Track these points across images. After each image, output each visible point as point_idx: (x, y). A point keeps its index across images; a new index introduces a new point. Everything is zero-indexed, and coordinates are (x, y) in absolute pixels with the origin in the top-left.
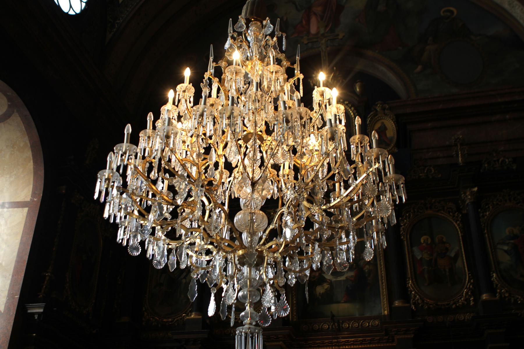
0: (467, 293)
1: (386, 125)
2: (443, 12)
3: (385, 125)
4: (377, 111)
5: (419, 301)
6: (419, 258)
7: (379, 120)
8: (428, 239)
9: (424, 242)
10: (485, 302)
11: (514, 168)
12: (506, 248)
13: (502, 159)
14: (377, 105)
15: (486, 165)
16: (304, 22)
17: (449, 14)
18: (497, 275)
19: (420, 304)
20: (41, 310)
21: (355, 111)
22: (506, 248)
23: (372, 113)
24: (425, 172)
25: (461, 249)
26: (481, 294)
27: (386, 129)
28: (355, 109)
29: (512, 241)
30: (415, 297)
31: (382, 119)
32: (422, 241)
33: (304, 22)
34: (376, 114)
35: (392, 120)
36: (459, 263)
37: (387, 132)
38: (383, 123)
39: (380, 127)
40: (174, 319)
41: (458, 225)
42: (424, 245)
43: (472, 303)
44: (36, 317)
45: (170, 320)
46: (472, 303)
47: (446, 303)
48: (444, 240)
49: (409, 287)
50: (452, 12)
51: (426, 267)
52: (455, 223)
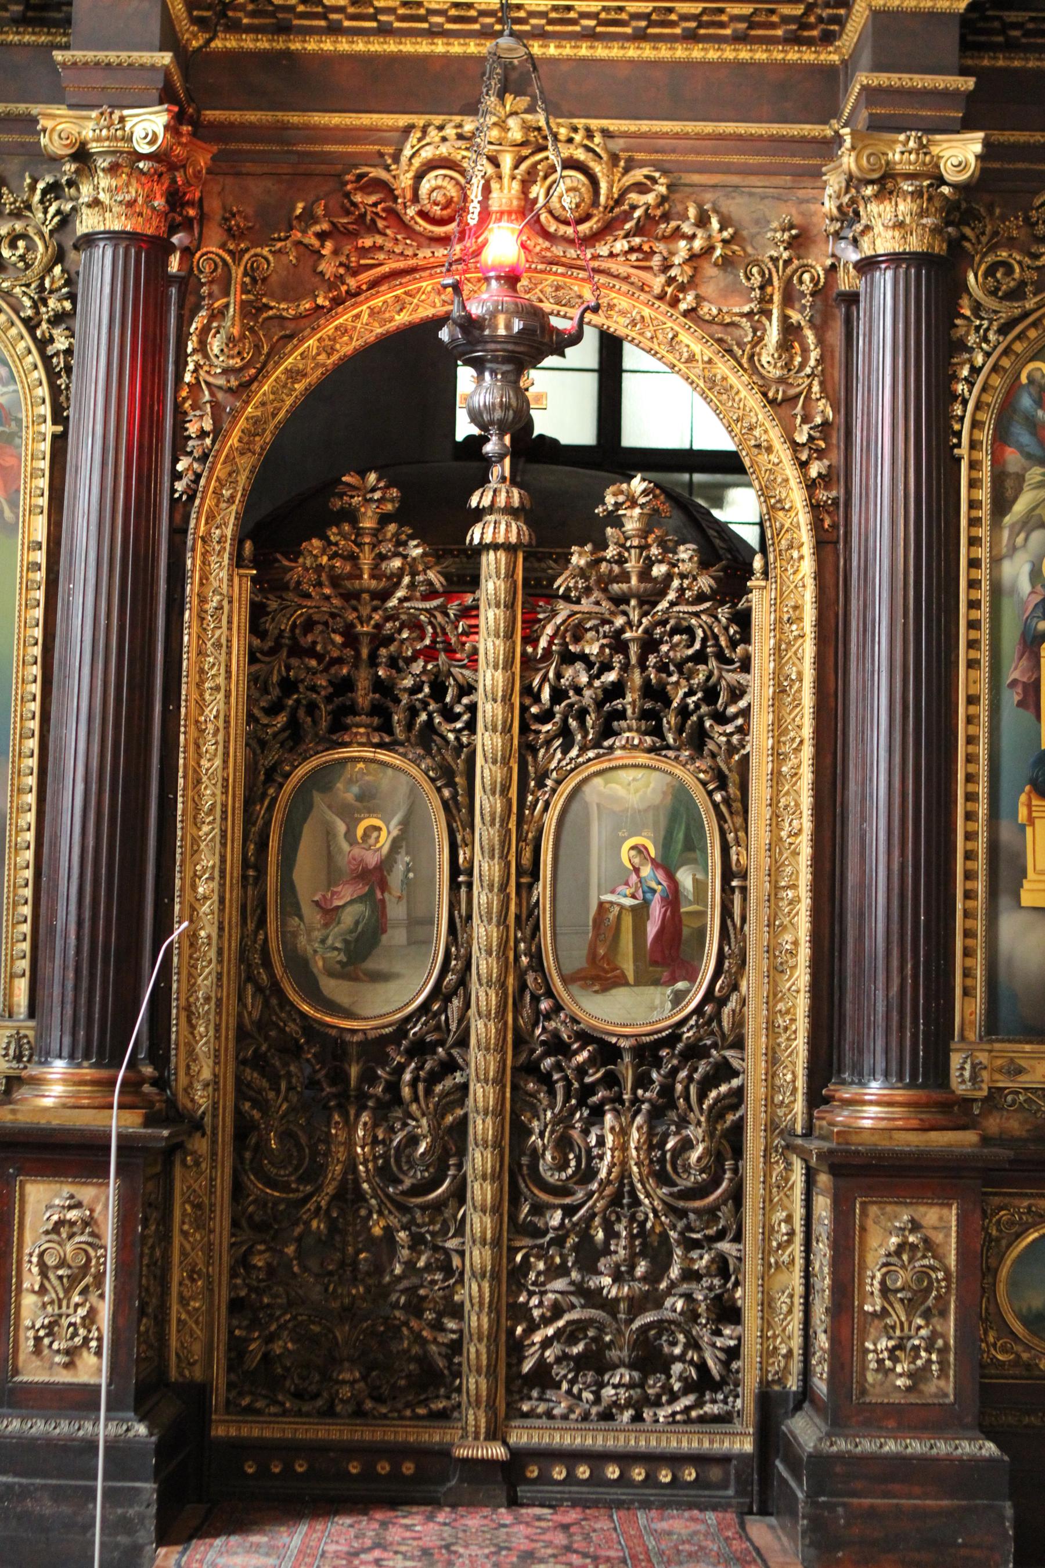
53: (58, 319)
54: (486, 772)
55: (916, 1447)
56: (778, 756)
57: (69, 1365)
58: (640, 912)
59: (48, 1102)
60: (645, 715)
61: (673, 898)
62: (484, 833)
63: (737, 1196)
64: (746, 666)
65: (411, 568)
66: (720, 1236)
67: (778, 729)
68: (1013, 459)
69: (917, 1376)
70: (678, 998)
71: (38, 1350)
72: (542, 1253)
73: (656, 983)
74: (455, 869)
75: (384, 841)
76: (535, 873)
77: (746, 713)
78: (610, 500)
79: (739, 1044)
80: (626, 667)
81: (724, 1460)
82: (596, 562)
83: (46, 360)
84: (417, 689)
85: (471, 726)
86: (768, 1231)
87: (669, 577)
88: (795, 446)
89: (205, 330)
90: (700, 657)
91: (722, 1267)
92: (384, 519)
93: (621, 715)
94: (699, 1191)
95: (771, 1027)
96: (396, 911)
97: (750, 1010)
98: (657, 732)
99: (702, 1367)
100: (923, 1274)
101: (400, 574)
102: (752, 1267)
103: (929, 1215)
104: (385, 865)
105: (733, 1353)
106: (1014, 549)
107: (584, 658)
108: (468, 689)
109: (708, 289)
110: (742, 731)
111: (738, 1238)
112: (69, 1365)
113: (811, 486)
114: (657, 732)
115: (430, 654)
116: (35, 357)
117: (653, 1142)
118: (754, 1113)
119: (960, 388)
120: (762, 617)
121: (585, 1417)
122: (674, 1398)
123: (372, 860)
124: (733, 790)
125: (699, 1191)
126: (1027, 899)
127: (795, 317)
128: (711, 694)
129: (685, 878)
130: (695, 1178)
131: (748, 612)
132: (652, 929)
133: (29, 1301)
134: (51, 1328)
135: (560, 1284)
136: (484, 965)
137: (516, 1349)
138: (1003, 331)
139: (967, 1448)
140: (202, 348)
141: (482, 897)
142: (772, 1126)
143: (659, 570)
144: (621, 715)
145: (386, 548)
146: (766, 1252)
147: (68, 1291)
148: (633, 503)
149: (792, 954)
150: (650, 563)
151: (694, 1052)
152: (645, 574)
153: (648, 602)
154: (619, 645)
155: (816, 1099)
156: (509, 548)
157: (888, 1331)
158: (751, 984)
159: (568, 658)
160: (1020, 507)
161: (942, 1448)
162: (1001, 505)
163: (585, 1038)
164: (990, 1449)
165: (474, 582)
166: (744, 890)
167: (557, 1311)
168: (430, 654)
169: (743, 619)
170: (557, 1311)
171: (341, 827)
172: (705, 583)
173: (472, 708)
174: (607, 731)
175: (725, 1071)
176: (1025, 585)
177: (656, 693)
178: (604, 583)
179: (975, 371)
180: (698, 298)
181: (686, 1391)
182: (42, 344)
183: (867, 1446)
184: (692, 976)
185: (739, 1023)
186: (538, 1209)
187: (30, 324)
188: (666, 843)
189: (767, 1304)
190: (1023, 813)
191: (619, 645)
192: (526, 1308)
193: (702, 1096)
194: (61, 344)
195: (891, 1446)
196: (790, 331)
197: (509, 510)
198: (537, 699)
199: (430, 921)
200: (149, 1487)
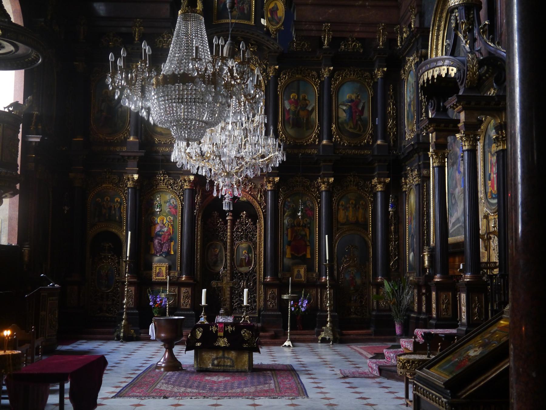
0: (315, 136)
3: (277, 6)
5: (284, 139)
6: (288, 109)
8: (295, 96)
9: (293, 98)
10: (324, 145)
11: (361, 51)
12: (345, 108)
13: (355, 43)
15: (343, 47)
18: (336, 125)
19: (284, 140)
20: (38, 140)
22: (345, 108)
25: (316, 105)
26: (323, 140)
27: (277, 9)
29: (349, 104)
30: (282, 135)
32: (291, 97)
35: (283, 2)
36: (313, 116)
37: (278, 12)
38: (276, 4)
39: (274, 7)
40: (114, 138)
41: (317, 88)
42: (293, 100)
43: (317, 143)
44: (34, 144)
45: (111, 138)
46: (317, 143)
47: (301, 141)
48: (306, 98)
49: (279, 128)
51: (291, 116)
52: (315, 87)
53: (181, 195)
54: (228, 244)
55: (273, 313)
56: (260, 242)
57: (186, 306)
58: (245, 259)
59: (183, 279)
60: (245, 238)
61: (249, 257)
62: (228, 251)
63: (256, 288)
64: (256, 232)
65: (220, 222)
66: (254, 294)
67: (260, 239)
68: (285, 209)
69: (273, 306)
70: (250, 268)
71: (183, 305)
72: (235, 296)
73: (247, 266)
74: (225, 255)
75: (218, 251)
76: (234, 255)
77: (256, 237)
78: (242, 214)
79: (256, 273)
80: (243, 232)
81: (255, 317)
82: (240, 221)
83: (180, 200)
84: (221, 235)
85: (227, 239)
86: (259, 293)
87: (248, 222)
88: (261, 208)
89: (197, 196)
90: (252, 231)
91: (254, 297)
92: (217, 217)
93: (243, 238)
94: (252, 288)
95: (259, 271)
96: (219, 259)
97: (257, 269)
98: (247, 239)
99: (252, 307)
100: (273, 296)
101: (219, 222)
102: (257, 297)
103: (274, 290)
104: (218, 254)
105: (256, 306)
106: (285, 219)
107: (239, 231)
108: (227, 235)
109: (252, 191)
110: (256, 239)
111: (256, 294)
112: (186, 306)
113: (263, 212)
114: (247, 239)
115: (222, 231)
116: (179, 199)
117: (247, 284)
118: (257, 280)
119: (280, 201)
120: (258, 227)
121: (240, 313)
122: (249, 311)
123: (216, 254)
124: (255, 246)
125: (252, 288)
126: (287, 257)
127: (262, 194)
128: (253, 235)
129: (250, 255)
130: (252, 287)
131: (257, 226)
132: (247, 261)
133: (182, 300)
134: (184, 303)
135: (237, 299)
136: (228, 265)
137: (233, 306)
138: (284, 195)
139: (278, 313)
140: (197, 198)
141: (228, 257)
142: (260, 282)
143: (247, 222)
144: (243, 238)
145: (217, 220)
146: (259, 295)
147: (186, 299)
148: (244, 215)
149: (262, 263)
150: (246, 221)
151: (251, 274)
152: (245, 222)
153: (246, 225)
154: (242, 230)
155: (264, 279)
156: (230, 220)
157: (270, 302)
158: (257, 266)
159: (237, 231)
160: (286, 214)
161: (275, 313)
162: (284, 214)
163: (240, 272)
164: (280, 313)
165: (227, 223)
166: (256, 256)
167: (237, 302)
168: (222, 231)
169: (256, 227)
170: (237, 302)
171: (213, 250)
172: (252, 223)
173: (227, 237)
174: (242, 239)
175: (255, 276)
176: (286, 223)
177: (247, 235)
178: (241, 223)
179: (281, 200)
180: (251, 192)
181: (250, 310)
182: (180, 198)
183: (268, 313)
184: (251, 265)
185: (256, 270)
186: (235, 291)
187: (178, 196)
188: (248, 251)
189: (259, 301)
190: (286, 248)
191: (242, 230)
192: (233, 302)
193: (252, 278)
194: (182, 198)
195: (270, 313)
196: (261, 196)
197: (231, 216)
198: (234, 236)
199: (223, 260)
200: (194, 318)
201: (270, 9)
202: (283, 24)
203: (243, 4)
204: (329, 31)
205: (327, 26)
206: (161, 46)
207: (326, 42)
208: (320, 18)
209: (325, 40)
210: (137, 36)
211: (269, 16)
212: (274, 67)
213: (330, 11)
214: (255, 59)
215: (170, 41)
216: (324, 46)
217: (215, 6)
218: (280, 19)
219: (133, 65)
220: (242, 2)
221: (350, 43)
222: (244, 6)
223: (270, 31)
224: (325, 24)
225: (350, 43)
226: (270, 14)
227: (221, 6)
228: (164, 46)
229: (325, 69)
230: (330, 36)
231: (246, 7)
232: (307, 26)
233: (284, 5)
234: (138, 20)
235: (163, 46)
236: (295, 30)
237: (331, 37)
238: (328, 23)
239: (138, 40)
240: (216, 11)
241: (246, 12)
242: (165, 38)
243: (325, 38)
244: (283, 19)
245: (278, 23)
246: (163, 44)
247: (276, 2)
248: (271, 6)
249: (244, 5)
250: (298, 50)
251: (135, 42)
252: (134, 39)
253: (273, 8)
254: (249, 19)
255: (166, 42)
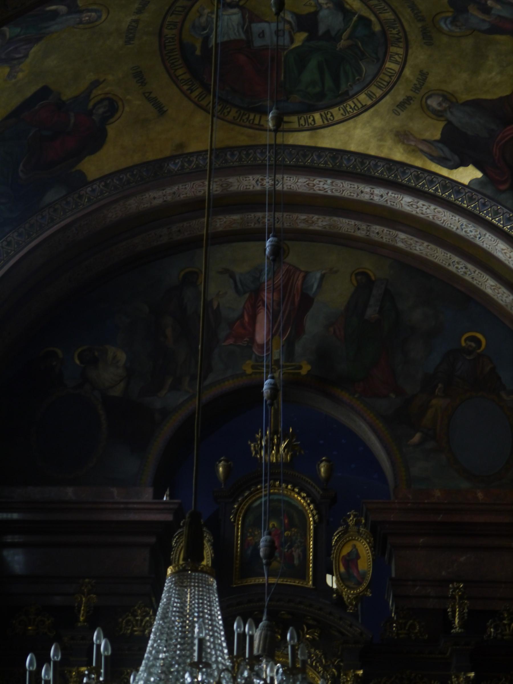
1: (359, 551)
2: (466, 340)
3: (357, 550)
4: (348, 526)
7: (349, 541)
14: (349, 516)
15: (492, 630)
16: (246, 319)
17: (473, 345)
21: (315, 512)
23: (340, 529)
24: (407, 628)
27: (358, 557)
28: (316, 508)
31: (354, 540)
33: (246, 319)
34: (345, 532)
35: (368, 543)
37: (359, 561)
38: (354, 546)
39: (351, 551)
50: (478, 342)
201: (343, 557)
202: (368, 587)
203: (290, 547)
204: (461, 598)
205: (458, 588)
206: (129, 631)
207: (457, 621)
208: (444, 573)
209: (454, 617)
210: (82, 612)
211: (342, 569)
212: (354, 672)
213: (463, 559)
214: (316, 655)
215: (147, 621)
216: (453, 628)
217: (237, 551)
218: (363, 576)
219: (71, 672)
220: (289, 544)
221: (505, 622)
222: (292, 551)
223: (345, 599)
224: (453, 584)
225: (505, 622)
226: (344, 565)
227: (249, 552)
228: (136, 631)
229: (458, 677)
230: (464, 609)
231: (296, 553)
232: (418, 588)
233: (370, 548)
234: (87, 580)
235: (133, 631)
236: (395, 596)
237: (466, 610)
238: (459, 582)
239: (84, 621)
240: (238, 562)
241: (296, 562)
242: (137, 616)
243: (454, 612)
244: (369, 576)
245: (360, 584)
246: (133, 627)
247: (354, 542)
248: (346, 551)
249: (293, 549)
250: (401, 636)
251: (79, 624)
252: (77, 620)
253: (349, 554)
254: (303, 576)
255: (139, 623)
